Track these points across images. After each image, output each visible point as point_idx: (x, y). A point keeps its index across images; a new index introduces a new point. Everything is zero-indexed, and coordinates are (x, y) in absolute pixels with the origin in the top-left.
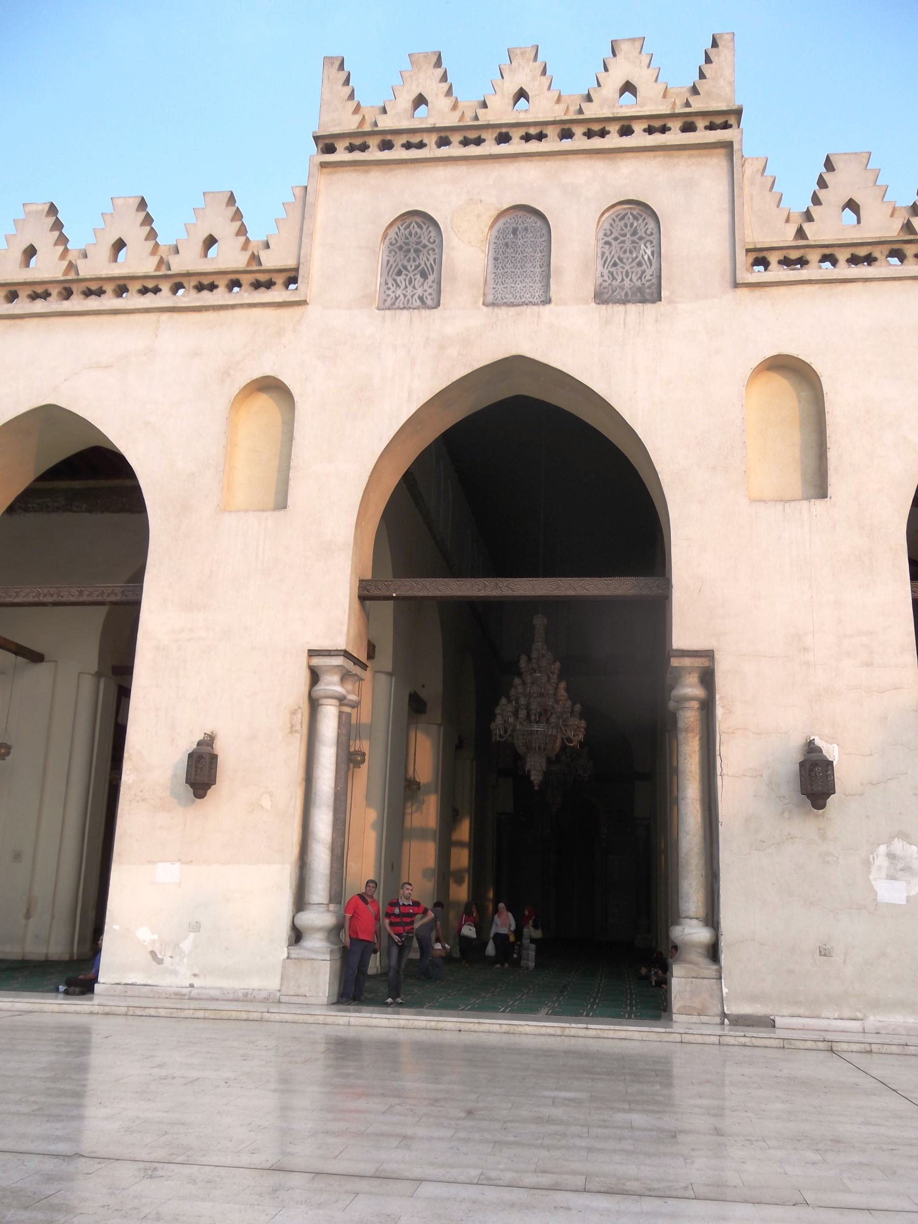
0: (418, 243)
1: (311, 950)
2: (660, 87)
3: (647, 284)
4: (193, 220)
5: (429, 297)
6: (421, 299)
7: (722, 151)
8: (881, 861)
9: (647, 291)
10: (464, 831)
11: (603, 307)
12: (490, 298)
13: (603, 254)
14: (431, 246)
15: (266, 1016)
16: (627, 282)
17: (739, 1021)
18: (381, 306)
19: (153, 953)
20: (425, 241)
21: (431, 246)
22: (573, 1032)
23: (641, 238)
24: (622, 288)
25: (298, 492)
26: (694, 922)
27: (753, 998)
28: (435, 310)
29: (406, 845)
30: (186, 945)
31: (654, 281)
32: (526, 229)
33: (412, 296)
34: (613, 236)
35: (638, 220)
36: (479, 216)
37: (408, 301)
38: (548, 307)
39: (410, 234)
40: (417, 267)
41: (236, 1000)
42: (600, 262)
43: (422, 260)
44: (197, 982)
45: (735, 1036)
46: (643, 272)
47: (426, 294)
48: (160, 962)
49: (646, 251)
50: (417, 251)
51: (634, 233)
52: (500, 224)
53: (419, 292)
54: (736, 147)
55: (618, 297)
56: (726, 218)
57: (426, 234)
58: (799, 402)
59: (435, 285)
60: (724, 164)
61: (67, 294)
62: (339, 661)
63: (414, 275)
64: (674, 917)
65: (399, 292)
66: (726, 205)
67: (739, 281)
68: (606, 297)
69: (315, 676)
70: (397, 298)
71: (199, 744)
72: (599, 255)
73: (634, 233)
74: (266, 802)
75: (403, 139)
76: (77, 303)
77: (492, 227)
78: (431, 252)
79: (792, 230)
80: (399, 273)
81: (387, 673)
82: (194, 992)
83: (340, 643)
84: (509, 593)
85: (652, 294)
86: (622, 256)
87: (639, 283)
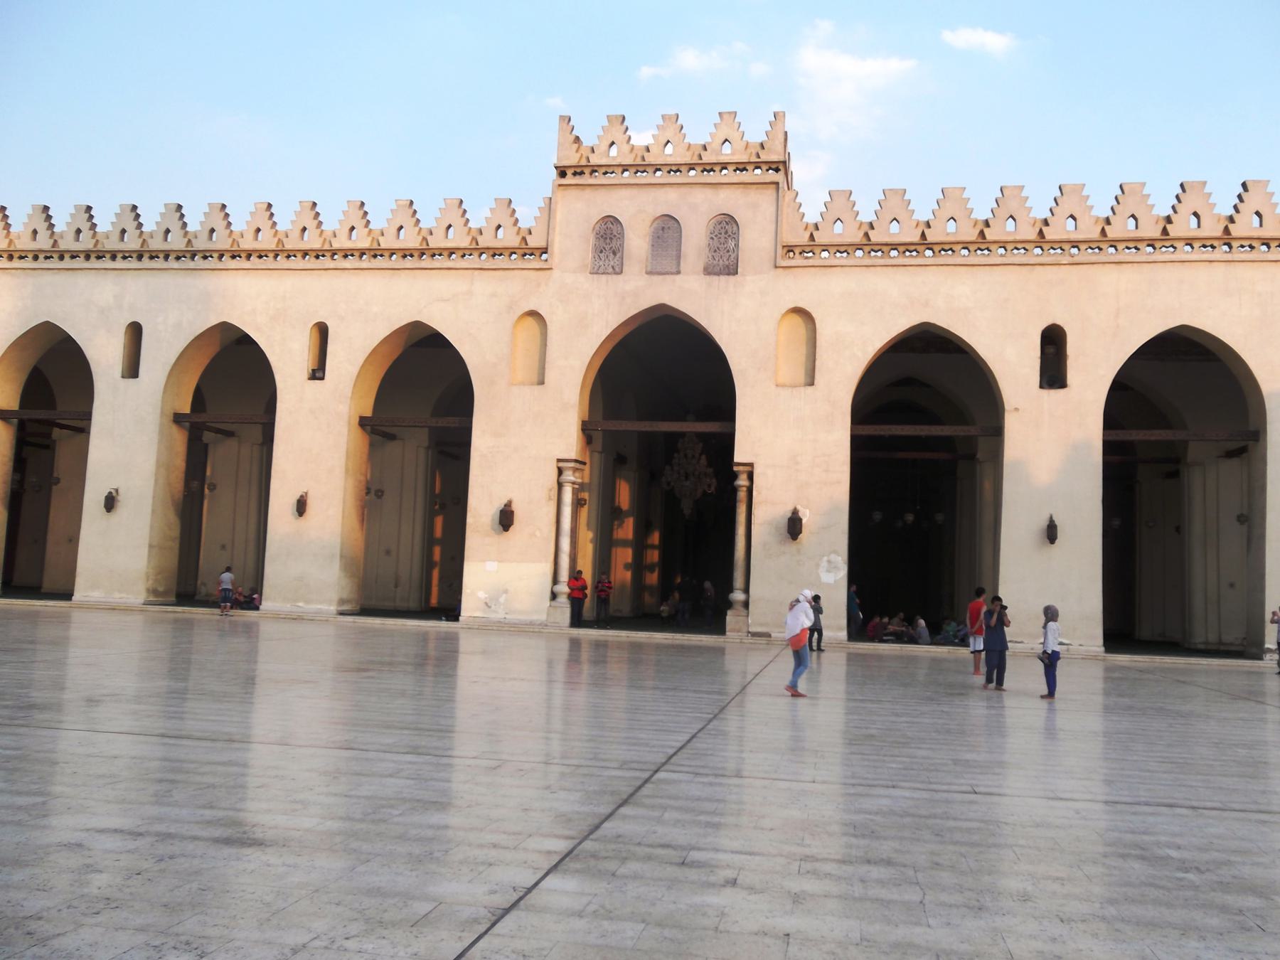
0: (612, 234)
1: (561, 603)
2: (744, 144)
3: (731, 263)
6: (613, 267)
7: (774, 186)
8: (824, 564)
10: (655, 538)
11: (708, 277)
12: (649, 269)
13: (709, 244)
14: (618, 236)
15: (542, 630)
16: (721, 261)
19: (486, 604)
21: (618, 236)
22: (678, 638)
23: (729, 236)
24: (718, 265)
25: (550, 376)
26: (738, 591)
27: (761, 625)
29: (614, 550)
30: (502, 600)
31: (735, 261)
37: (606, 268)
38: (677, 277)
40: (611, 248)
41: (527, 625)
43: (613, 244)
44: (507, 616)
45: (750, 640)
46: (730, 256)
48: (490, 607)
50: (611, 239)
51: (726, 233)
53: (612, 263)
54: (780, 185)
56: (773, 226)
58: (807, 330)
59: (620, 260)
62: (572, 465)
64: (731, 589)
65: (601, 263)
66: (774, 219)
67: (777, 265)
68: (709, 270)
69: (560, 471)
71: (505, 506)
73: (726, 233)
74: (538, 533)
75: (603, 170)
76: (426, 262)
77: (651, 226)
79: (807, 235)
80: (601, 252)
81: (599, 452)
82: (507, 621)
83: (573, 456)
84: (656, 429)
85: (733, 269)
87: (727, 263)
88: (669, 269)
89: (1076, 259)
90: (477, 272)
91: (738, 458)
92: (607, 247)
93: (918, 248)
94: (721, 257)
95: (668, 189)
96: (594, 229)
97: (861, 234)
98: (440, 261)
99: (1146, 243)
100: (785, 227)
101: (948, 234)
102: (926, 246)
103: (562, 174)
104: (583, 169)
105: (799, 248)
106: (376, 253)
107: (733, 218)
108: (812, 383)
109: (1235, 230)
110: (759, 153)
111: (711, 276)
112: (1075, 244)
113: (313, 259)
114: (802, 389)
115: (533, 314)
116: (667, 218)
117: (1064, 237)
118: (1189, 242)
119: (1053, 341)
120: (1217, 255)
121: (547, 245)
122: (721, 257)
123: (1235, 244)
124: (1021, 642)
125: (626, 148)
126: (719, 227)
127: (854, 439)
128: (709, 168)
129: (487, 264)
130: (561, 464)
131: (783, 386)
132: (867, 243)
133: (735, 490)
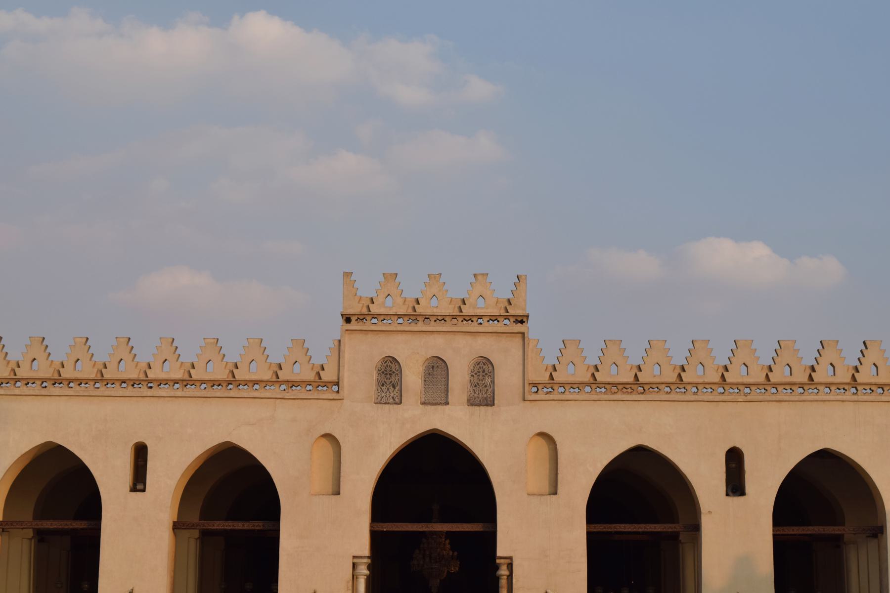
0: (391, 371)
3: (489, 396)
4: (288, 353)
5: (397, 397)
6: (393, 398)
7: (520, 335)
9: (489, 399)
12: (423, 400)
13: (470, 381)
14: (396, 372)
16: (480, 394)
18: (376, 401)
20: (394, 370)
23: (486, 374)
28: (400, 405)
32: (438, 367)
33: (389, 397)
34: (475, 373)
35: (485, 365)
38: (447, 407)
39: (387, 365)
40: (391, 382)
42: (469, 385)
46: (487, 390)
47: (395, 396)
51: (484, 371)
52: (426, 364)
53: (392, 395)
54: (526, 335)
55: (477, 402)
56: (521, 367)
57: (394, 366)
58: (549, 450)
59: (399, 392)
60: (521, 342)
63: (390, 386)
66: (521, 362)
69: (354, 566)
70: (382, 397)
72: (469, 381)
73: (484, 371)
78: (396, 375)
80: (383, 385)
85: (491, 401)
86: (478, 382)
87: (485, 396)
88: (439, 400)
89: (749, 398)
90: (278, 401)
91: (500, 552)
93: (633, 386)
94: (480, 392)
95: (436, 336)
96: (376, 366)
97: (589, 375)
98: (244, 391)
99: (798, 386)
100: (529, 367)
101: (655, 376)
102: (638, 385)
103: (348, 320)
104: (365, 316)
105: (543, 385)
106: (187, 382)
107: (489, 360)
108: (555, 493)
109: (860, 378)
110: (507, 307)
112: (748, 386)
113: (130, 388)
114: (548, 496)
115: (329, 437)
116: (435, 359)
117: (740, 380)
118: (828, 386)
119: (735, 458)
120: (848, 396)
121: (339, 379)
122: (480, 392)
123: (859, 388)
125: (400, 301)
127: (589, 534)
128: (469, 319)
129: (288, 394)
130: (356, 560)
131: (534, 495)
132: (594, 382)
133: (497, 579)
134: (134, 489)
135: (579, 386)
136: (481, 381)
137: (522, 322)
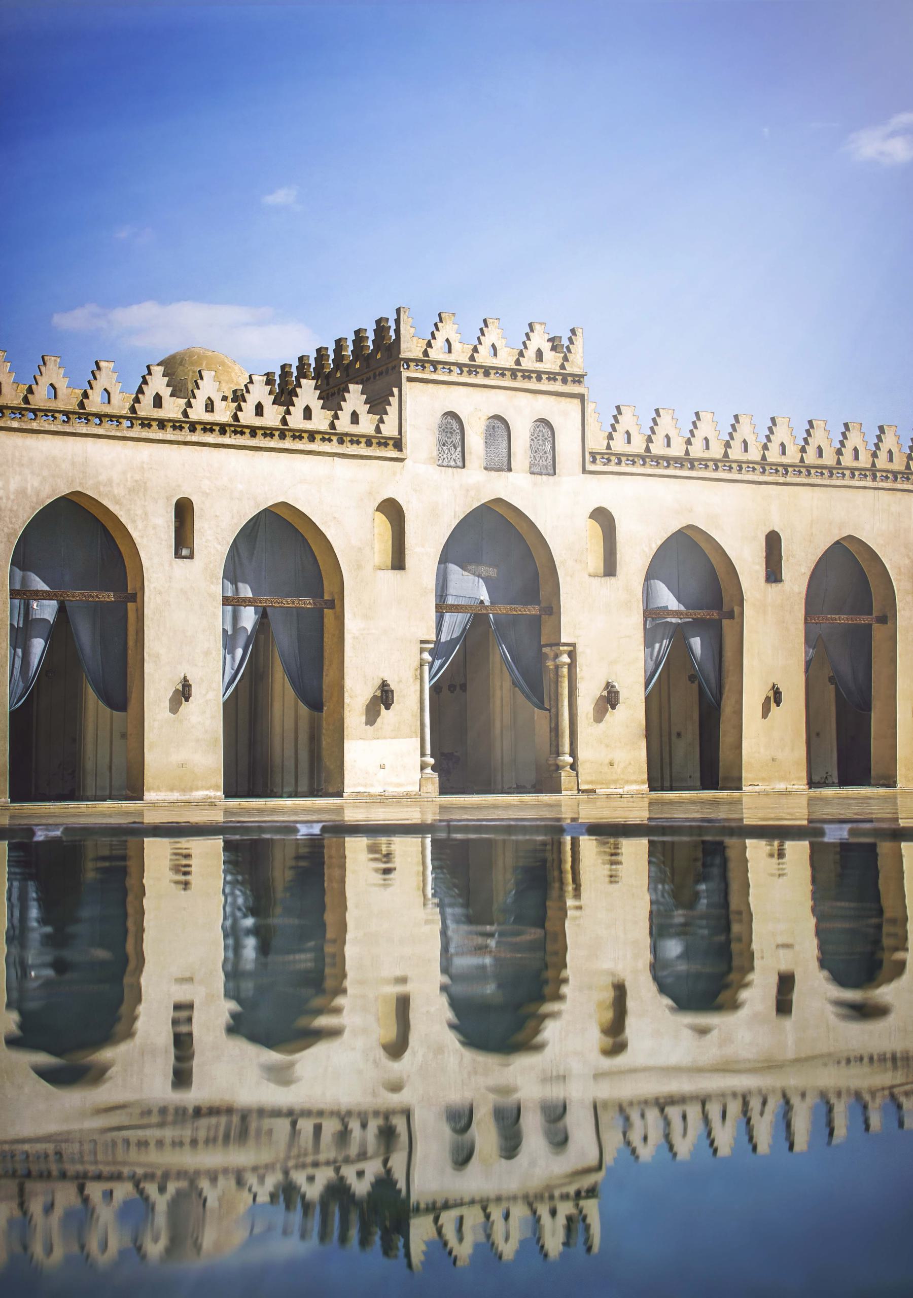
0: (452, 428)
3: (549, 464)
6: (454, 460)
13: (531, 445)
17: (584, 791)
25: (410, 560)
36: (479, 419)
40: (452, 442)
46: (547, 457)
49: (548, 447)
53: (454, 457)
59: (460, 454)
61: (283, 436)
69: (422, 651)
70: (444, 459)
80: (444, 445)
92: (449, 441)
111: (536, 476)
112: (786, 467)
124: (758, 785)
126: (538, 429)
134: (178, 555)
135: (632, 459)
136: (541, 447)
137: (580, 382)
